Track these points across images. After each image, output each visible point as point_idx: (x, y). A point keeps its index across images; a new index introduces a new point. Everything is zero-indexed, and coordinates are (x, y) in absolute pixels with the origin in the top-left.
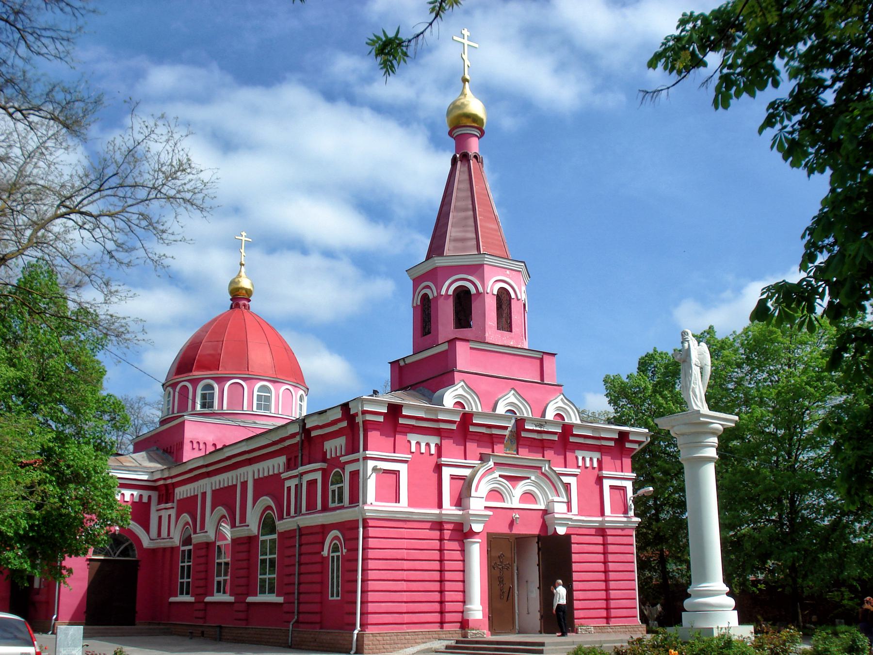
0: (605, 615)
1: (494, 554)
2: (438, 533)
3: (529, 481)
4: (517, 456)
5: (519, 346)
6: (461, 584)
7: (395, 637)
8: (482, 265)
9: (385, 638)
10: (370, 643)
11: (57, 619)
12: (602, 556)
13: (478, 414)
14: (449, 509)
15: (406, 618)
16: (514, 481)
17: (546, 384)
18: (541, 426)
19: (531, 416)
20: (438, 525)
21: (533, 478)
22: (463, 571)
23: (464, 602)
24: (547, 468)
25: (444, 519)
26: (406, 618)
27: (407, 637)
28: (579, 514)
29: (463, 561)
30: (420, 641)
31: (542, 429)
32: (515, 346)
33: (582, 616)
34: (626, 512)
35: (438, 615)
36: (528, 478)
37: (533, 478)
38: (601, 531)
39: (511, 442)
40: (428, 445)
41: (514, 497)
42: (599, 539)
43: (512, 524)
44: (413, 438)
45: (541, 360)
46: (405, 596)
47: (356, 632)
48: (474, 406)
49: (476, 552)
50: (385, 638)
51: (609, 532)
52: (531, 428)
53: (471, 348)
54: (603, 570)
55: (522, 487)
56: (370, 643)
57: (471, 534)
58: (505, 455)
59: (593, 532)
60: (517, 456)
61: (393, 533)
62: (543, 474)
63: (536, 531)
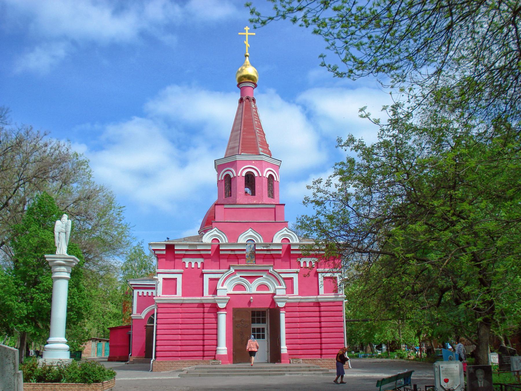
0: (320, 353)
1: (237, 319)
2: (202, 309)
3: (262, 278)
4: (255, 265)
5: (260, 203)
6: (215, 336)
7: (171, 364)
8: (236, 161)
9: (165, 364)
10: (156, 366)
11: (131, 355)
12: (318, 318)
13: (222, 244)
14: (207, 296)
15: (180, 354)
16: (251, 280)
17: (277, 222)
18: (267, 247)
19: (262, 242)
20: (202, 305)
21: (264, 276)
22: (217, 329)
23: (217, 345)
24: (271, 271)
25: (204, 302)
26: (180, 354)
27: (179, 363)
28: (299, 295)
29: (217, 323)
30: (186, 366)
31: (268, 249)
32: (257, 203)
33: (301, 353)
34: (336, 291)
35: (323, 353)
36: (262, 276)
37: (264, 276)
38: (318, 304)
39: (251, 257)
40: (196, 263)
41: (252, 288)
42: (317, 309)
43: (250, 303)
44: (187, 261)
45: (275, 208)
46: (179, 343)
47: (152, 360)
48: (224, 239)
49: (223, 318)
50: (165, 364)
51: (322, 304)
52: (260, 249)
53: (225, 208)
54: (319, 326)
55: (257, 282)
56: (156, 366)
57: (219, 309)
58: (246, 265)
59: (312, 304)
60: (255, 265)
61: (172, 310)
62: (270, 274)
63: (268, 306)
